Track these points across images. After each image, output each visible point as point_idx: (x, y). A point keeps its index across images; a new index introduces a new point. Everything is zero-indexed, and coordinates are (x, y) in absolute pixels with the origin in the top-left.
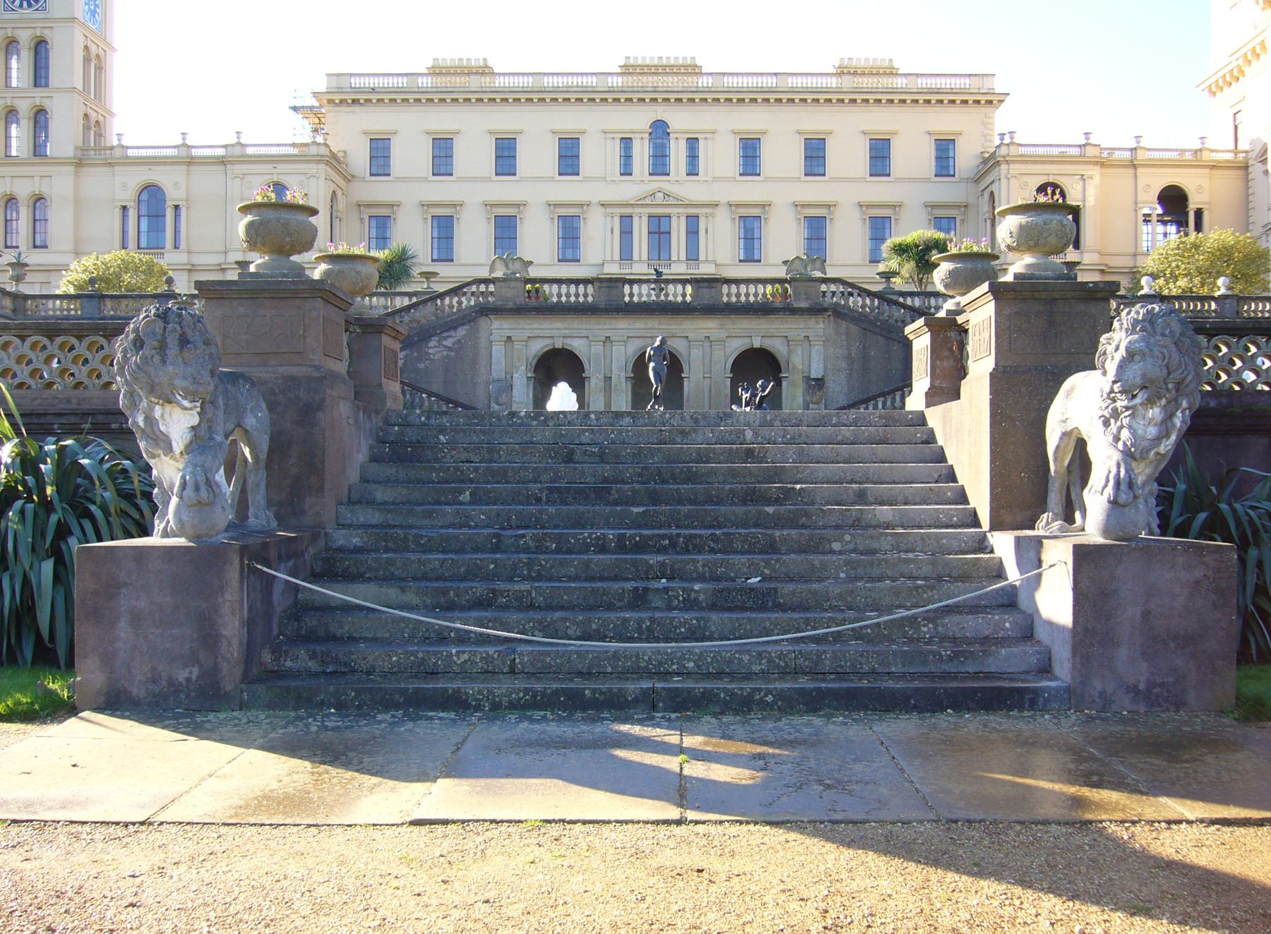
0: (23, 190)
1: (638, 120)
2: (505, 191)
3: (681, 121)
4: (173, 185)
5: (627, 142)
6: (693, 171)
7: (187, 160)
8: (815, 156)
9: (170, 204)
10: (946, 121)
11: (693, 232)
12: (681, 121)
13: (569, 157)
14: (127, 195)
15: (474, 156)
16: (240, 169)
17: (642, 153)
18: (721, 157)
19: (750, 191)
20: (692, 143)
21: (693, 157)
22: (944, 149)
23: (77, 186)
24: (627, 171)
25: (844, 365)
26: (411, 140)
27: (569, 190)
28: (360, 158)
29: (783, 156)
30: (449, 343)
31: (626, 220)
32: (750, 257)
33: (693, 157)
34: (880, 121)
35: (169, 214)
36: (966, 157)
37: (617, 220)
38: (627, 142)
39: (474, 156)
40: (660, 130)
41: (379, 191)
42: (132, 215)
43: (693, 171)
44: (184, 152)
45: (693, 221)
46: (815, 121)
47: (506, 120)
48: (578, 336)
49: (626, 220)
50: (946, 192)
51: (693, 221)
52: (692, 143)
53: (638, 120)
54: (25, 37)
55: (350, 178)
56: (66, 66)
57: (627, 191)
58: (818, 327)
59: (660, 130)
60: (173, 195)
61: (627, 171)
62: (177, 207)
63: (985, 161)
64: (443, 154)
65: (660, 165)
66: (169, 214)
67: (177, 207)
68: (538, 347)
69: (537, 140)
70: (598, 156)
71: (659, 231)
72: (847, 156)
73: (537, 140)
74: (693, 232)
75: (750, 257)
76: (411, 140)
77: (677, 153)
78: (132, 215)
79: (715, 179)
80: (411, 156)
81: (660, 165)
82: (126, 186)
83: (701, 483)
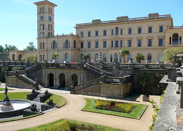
0: (42, 42)
1: (114, 27)
5: (112, 30)
6: (121, 34)
8: (140, 31)
12: (120, 27)
13: (105, 33)
18: (126, 32)
20: (122, 30)
23: (47, 41)
24: (112, 35)
25: (86, 77)
28: (80, 35)
30: (39, 72)
31: (112, 42)
34: (150, 24)
37: (111, 41)
38: (112, 30)
40: (117, 28)
41: (81, 39)
43: (121, 34)
44: (63, 36)
45: (121, 41)
48: (53, 71)
49: (112, 42)
51: (121, 41)
52: (122, 30)
57: (112, 37)
58: (82, 71)
59: (117, 28)
61: (112, 35)
65: (117, 33)
67: (57, 43)
68: (48, 73)
70: (109, 33)
71: (117, 42)
72: (145, 30)
79: (125, 35)
80: (86, 34)
81: (117, 33)
83: (125, 78)
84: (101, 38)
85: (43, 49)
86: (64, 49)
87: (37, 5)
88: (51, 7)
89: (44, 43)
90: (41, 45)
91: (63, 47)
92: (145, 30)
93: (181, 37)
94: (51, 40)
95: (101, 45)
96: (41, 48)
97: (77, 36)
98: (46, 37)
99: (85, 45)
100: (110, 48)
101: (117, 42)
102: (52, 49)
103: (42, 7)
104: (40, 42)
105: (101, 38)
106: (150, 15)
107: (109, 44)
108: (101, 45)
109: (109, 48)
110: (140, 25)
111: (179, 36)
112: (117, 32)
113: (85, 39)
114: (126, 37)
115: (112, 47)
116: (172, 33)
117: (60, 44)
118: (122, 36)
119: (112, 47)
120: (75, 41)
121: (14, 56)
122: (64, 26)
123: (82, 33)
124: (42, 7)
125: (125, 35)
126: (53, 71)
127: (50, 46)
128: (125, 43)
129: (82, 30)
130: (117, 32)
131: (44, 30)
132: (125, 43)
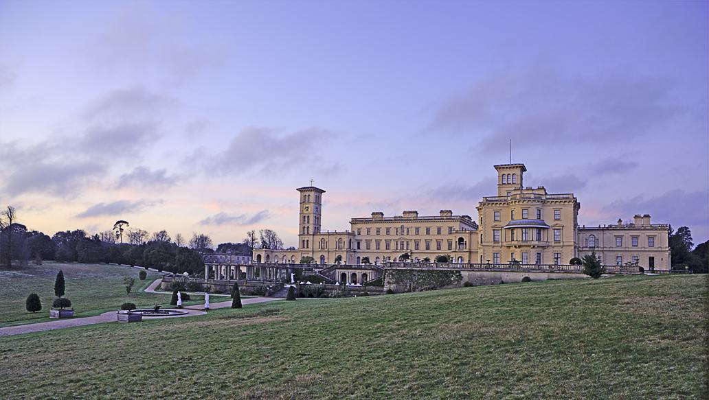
0: (306, 240)
3: (406, 225)
7: (329, 234)
8: (428, 231)
11: (407, 245)
17: (399, 231)
18: (413, 231)
19: (417, 237)
20: (408, 229)
27: (388, 238)
28: (356, 233)
41: (358, 238)
52: (408, 229)
53: (399, 225)
57: (397, 238)
70: (393, 232)
71: (402, 243)
72: (434, 231)
74: (407, 245)
80: (364, 232)
84: (383, 237)
85: (308, 250)
87: (301, 191)
88: (318, 194)
90: (304, 243)
92: (434, 231)
94: (318, 238)
95: (383, 245)
97: (353, 234)
99: (363, 245)
101: (402, 243)
105: (383, 237)
108: (383, 245)
110: (428, 225)
113: (363, 237)
114: (413, 238)
115: (397, 249)
117: (332, 241)
118: (408, 237)
120: (350, 240)
121: (259, 257)
122: (335, 219)
126: (346, 271)
129: (359, 226)
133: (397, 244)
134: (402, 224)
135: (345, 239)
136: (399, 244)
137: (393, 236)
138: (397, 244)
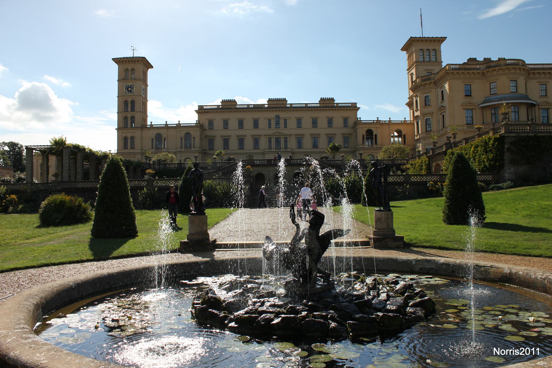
0: (129, 135)
2: (241, 132)
3: (282, 115)
4: (163, 133)
5: (270, 120)
6: (286, 127)
8: (315, 123)
9: (163, 138)
10: (346, 114)
11: (286, 141)
13: (256, 124)
14: (153, 136)
15: (233, 124)
16: (179, 129)
17: (273, 123)
18: (292, 123)
19: (299, 131)
20: (285, 120)
21: (285, 124)
22: (345, 120)
24: (270, 127)
26: (218, 120)
27: (256, 132)
28: (206, 125)
29: (307, 123)
31: (270, 139)
32: (300, 147)
33: (285, 124)
34: (330, 114)
35: (163, 140)
36: (351, 122)
38: (270, 120)
39: (233, 124)
40: (278, 117)
41: (210, 133)
42: (154, 141)
43: (286, 127)
45: (286, 139)
46: (315, 114)
47: (241, 115)
50: (346, 131)
51: (286, 139)
52: (285, 120)
54: (129, 100)
55: (205, 130)
56: (138, 107)
57: (270, 132)
59: (278, 117)
60: (164, 136)
61: (270, 127)
62: (165, 139)
63: (355, 123)
64: (226, 123)
66: (163, 140)
67: (165, 139)
69: (248, 119)
70: (263, 124)
71: (278, 141)
72: (322, 123)
73: (248, 119)
74: (286, 141)
75: (300, 147)
76: (218, 120)
77: (282, 122)
78: (154, 141)
79: (291, 129)
80: (218, 124)
82: (153, 134)
86: (183, 150)
89: (132, 138)
91: (179, 146)
93: (376, 135)
96: (152, 148)
98: (140, 126)
100: (267, 150)
101: (278, 141)
102: (154, 150)
103: (130, 68)
104: (124, 135)
105: (249, 131)
106: (322, 100)
107: (263, 144)
109: (266, 150)
111: (374, 134)
112: (278, 123)
113: (218, 131)
115: (270, 148)
116: (366, 129)
118: (285, 132)
119: (270, 148)
123: (211, 123)
124: (130, 68)
125: (291, 129)
127: (148, 144)
128: (292, 143)
130: (278, 123)
131: (134, 113)
132: (292, 143)
133: (270, 142)
134: (277, 113)
135: (196, 134)
136: (273, 141)
137: (263, 130)
138: (270, 142)
